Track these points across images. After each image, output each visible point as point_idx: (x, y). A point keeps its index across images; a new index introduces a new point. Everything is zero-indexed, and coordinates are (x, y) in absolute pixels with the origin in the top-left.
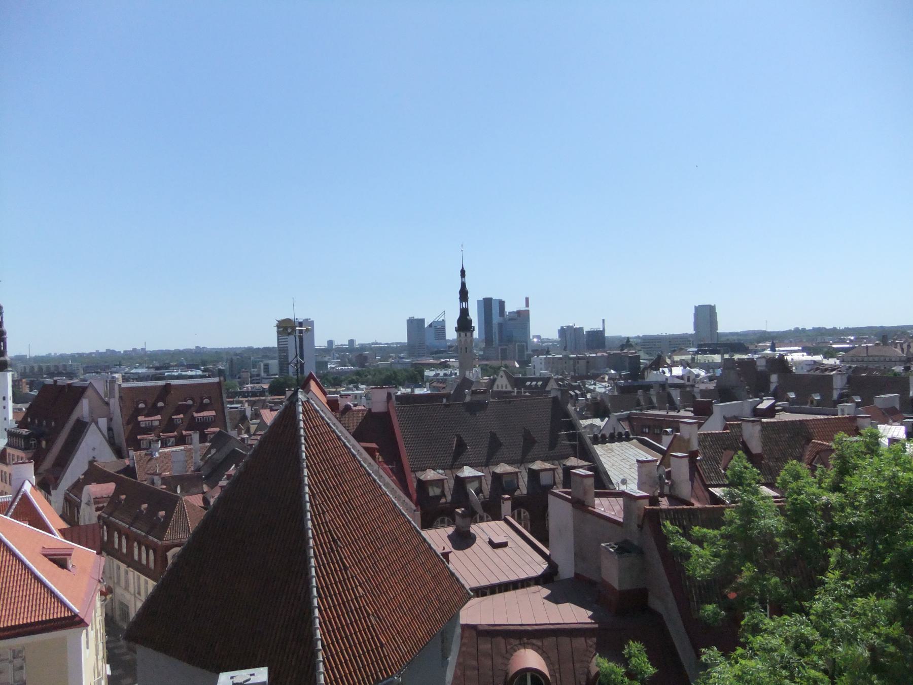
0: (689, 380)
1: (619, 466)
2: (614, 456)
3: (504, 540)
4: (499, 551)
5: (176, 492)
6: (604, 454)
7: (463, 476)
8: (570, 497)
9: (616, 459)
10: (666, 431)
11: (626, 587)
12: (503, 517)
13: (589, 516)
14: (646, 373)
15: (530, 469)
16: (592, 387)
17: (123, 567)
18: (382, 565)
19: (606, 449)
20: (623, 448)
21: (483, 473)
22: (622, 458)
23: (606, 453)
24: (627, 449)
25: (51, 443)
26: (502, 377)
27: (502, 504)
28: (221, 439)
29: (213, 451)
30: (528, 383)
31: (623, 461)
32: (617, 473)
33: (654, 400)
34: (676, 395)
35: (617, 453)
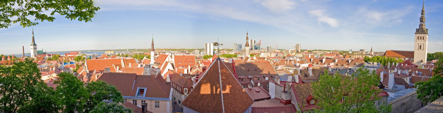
3: (259, 91)
4: (258, 93)
5: (185, 77)
11: (287, 100)
17: (175, 90)
18: (236, 95)
25: (161, 65)
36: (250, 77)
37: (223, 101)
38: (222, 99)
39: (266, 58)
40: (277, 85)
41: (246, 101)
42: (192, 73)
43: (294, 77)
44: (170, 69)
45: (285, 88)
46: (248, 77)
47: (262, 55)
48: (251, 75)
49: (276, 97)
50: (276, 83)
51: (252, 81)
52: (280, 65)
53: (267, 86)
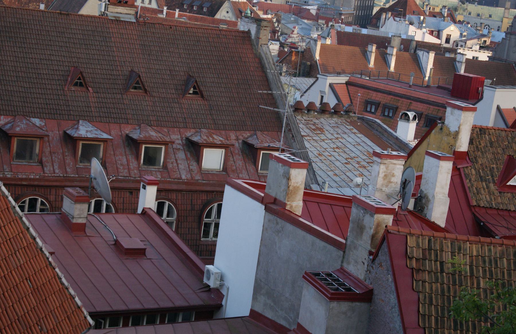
1: (329, 158)
2: (323, 140)
3: (140, 245)
4: (131, 264)
6: (308, 136)
7: (76, 135)
8: (263, 195)
9: (326, 146)
10: (407, 115)
12: (140, 211)
13: (289, 227)
14: (384, 16)
15: (188, 139)
16: (291, 26)
19: (314, 127)
20: (340, 131)
21: (110, 135)
22: (335, 146)
23: (311, 134)
24: (345, 133)
27: (142, 190)
31: (337, 150)
32: (324, 168)
35: (330, 136)
43: (419, 178)
48: (90, 119)
49: (259, 309)
50: (275, 201)
53: (209, 216)
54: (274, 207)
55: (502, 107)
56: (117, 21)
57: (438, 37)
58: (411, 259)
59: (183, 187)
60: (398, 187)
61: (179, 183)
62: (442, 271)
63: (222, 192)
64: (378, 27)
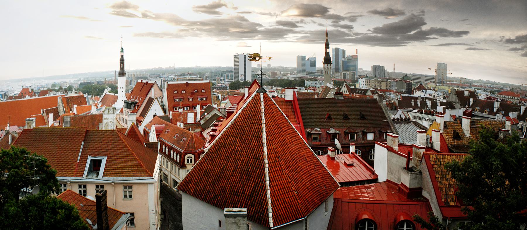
0: (434, 97)
5: (190, 130)
12: (350, 153)
13: (395, 155)
14: (415, 91)
16: (388, 96)
18: (299, 170)
26: (344, 87)
28: (211, 109)
29: (206, 114)
30: (357, 91)
33: (419, 104)
34: (429, 103)
36: (332, 131)
37: (268, 183)
38: (267, 178)
39: (369, 91)
40: (393, 153)
41: (322, 185)
42: (204, 122)
43: (431, 137)
44: (157, 115)
45: (409, 160)
46: (328, 132)
47: (362, 83)
48: (334, 128)
51: (336, 141)
52: (400, 108)
54: (390, 149)
55: (452, 115)
56: (338, 99)
57: (431, 96)
58: (431, 161)
59: (362, 145)
60: (425, 141)
61: (360, 144)
62: (440, 164)
63: (374, 146)
64: (413, 94)
